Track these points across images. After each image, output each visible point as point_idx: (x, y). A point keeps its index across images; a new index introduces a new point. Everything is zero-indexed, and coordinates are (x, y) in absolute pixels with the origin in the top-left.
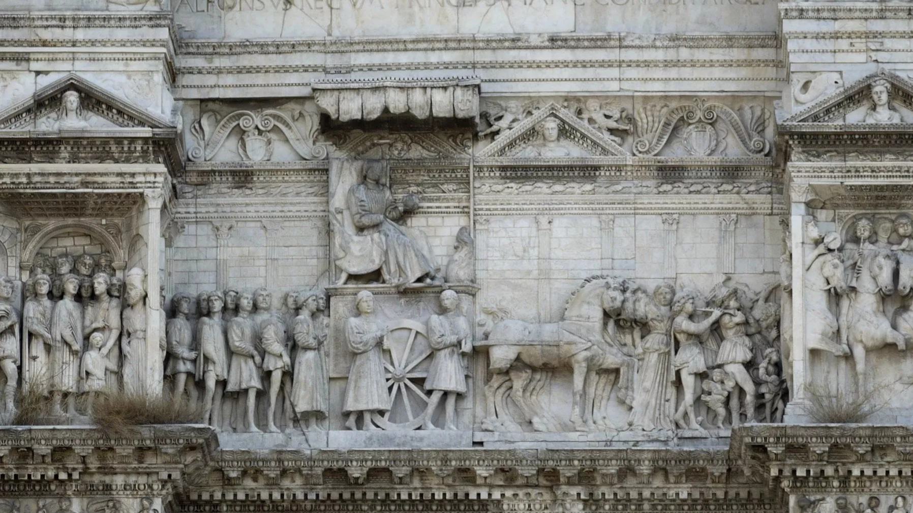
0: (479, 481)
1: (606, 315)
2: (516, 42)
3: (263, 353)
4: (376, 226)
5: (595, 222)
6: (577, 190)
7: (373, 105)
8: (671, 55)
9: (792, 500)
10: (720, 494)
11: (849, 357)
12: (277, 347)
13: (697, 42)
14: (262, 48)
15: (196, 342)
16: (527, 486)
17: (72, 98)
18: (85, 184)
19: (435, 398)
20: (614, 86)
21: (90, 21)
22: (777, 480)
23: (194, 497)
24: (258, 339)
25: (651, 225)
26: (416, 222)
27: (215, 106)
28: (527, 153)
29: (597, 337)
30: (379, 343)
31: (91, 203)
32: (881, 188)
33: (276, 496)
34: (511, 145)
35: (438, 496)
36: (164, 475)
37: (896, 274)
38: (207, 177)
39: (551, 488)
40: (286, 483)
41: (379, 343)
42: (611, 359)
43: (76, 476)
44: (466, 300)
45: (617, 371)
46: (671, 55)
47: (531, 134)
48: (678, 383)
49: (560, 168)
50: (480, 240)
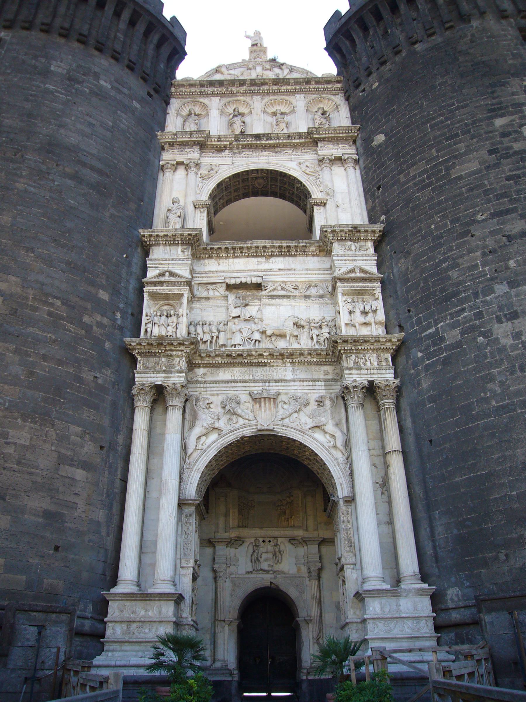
0: (265, 357)
1: (294, 324)
2: (271, 270)
3: (212, 332)
4: (239, 307)
5: (290, 307)
6: (286, 301)
7: (238, 281)
8: (306, 272)
9: (344, 356)
10: (324, 360)
11: (354, 326)
12: (215, 331)
13: (313, 270)
14: (213, 272)
15: (196, 331)
16: (277, 359)
17: (167, 274)
18: (169, 291)
19: (253, 341)
20: (294, 279)
21: (173, 259)
22: (340, 350)
23: (194, 362)
24: (210, 330)
25: (303, 307)
26: (248, 307)
27: (202, 285)
28: (274, 293)
29: (292, 328)
30: (240, 330)
31: (171, 296)
32: (359, 290)
33: (214, 362)
34: (270, 291)
35: (255, 362)
36: (185, 351)
37: (364, 308)
38: (200, 299)
39: (282, 359)
40: (217, 359)
41: (240, 330)
42: (295, 334)
43: (163, 351)
44: (260, 322)
45: (297, 336)
46: (306, 272)
47: (274, 290)
48: (312, 338)
49: (282, 296)
50: (263, 311)
